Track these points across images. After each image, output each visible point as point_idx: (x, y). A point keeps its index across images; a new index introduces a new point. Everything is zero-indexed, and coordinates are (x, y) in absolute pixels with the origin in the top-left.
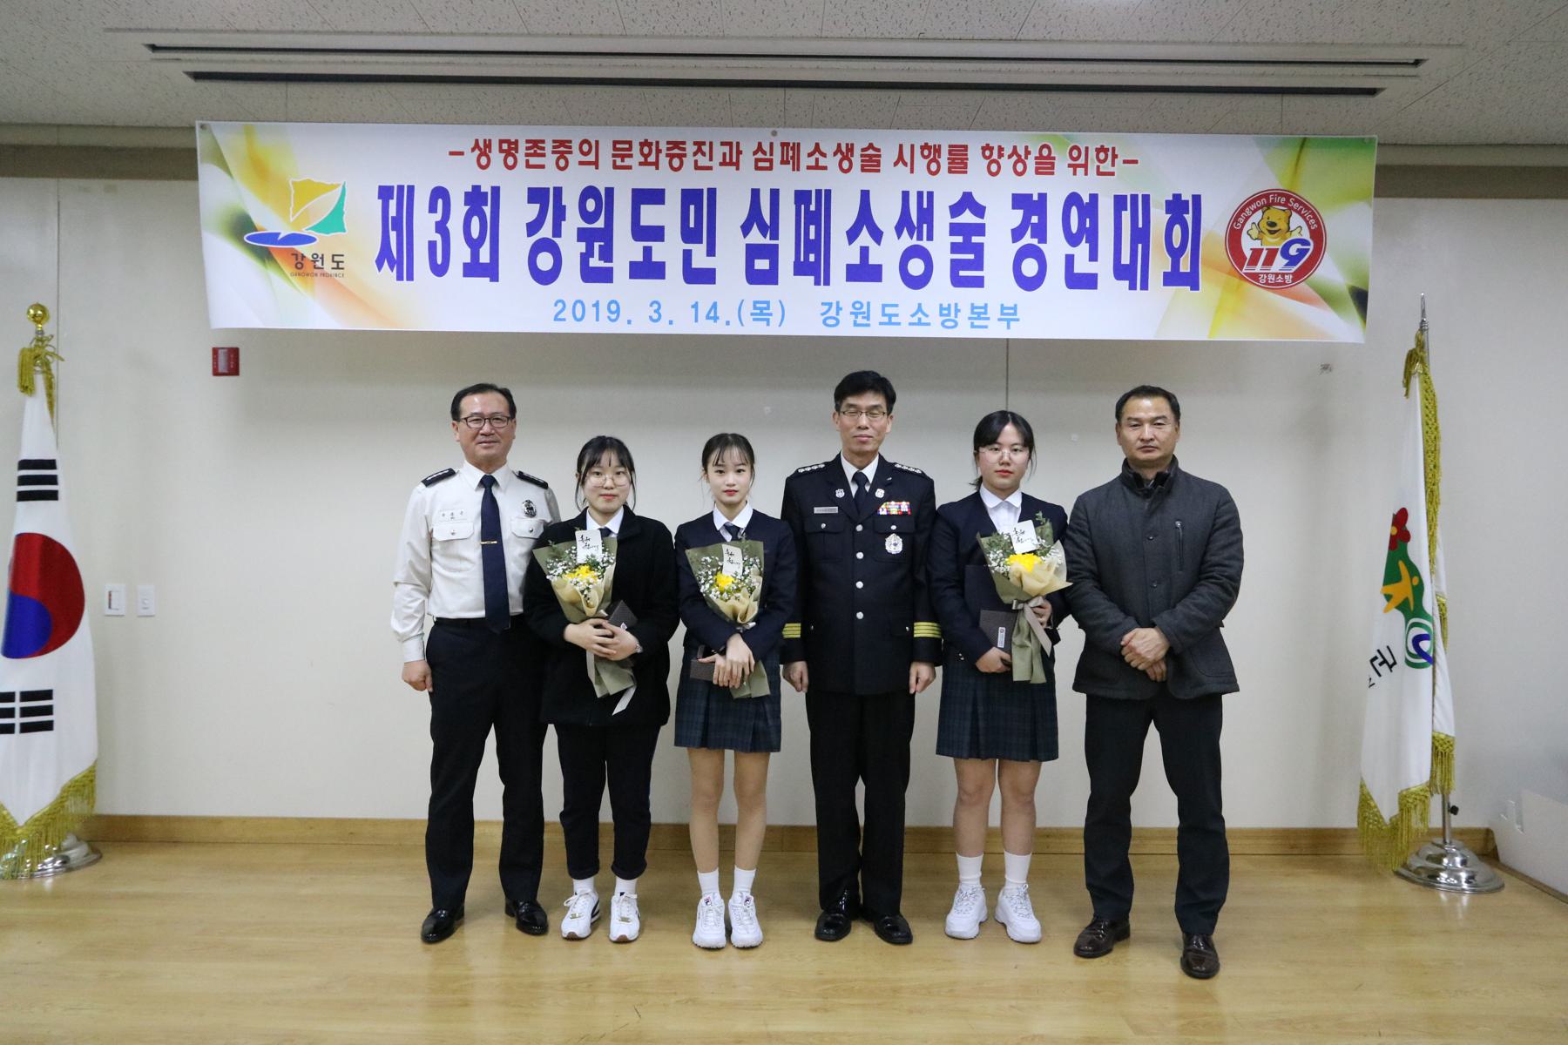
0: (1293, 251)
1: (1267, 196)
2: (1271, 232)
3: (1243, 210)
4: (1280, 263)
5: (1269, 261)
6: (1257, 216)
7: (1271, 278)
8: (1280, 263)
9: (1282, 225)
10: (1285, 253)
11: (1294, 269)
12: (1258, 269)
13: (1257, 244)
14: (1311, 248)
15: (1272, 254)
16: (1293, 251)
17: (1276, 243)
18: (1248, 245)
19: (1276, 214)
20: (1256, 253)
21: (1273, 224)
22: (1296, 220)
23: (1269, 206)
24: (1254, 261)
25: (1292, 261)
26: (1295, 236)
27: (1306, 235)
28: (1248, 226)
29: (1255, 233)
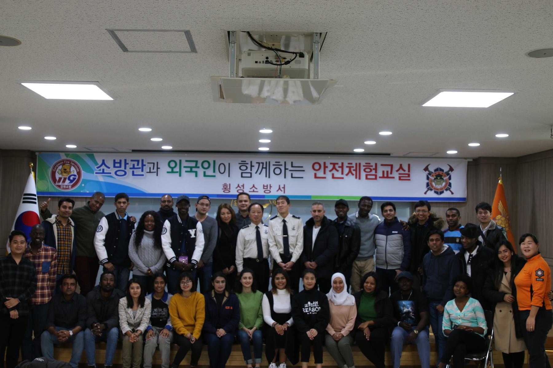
0: (71, 178)
1: (63, 161)
2: (65, 172)
3: (55, 165)
4: (67, 182)
5: (64, 181)
6: (60, 167)
7: (65, 187)
8: (67, 182)
9: (68, 170)
10: (69, 179)
11: (72, 184)
12: (61, 184)
13: (61, 176)
14: (77, 177)
15: (65, 179)
16: (71, 178)
17: (66, 175)
18: (58, 176)
19: (67, 166)
20: (60, 179)
21: (65, 170)
22: (73, 169)
23: (64, 164)
24: (59, 181)
25: (71, 181)
26: (72, 173)
27: (75, 173)
28: (57, 170)
29: (60, 172)
